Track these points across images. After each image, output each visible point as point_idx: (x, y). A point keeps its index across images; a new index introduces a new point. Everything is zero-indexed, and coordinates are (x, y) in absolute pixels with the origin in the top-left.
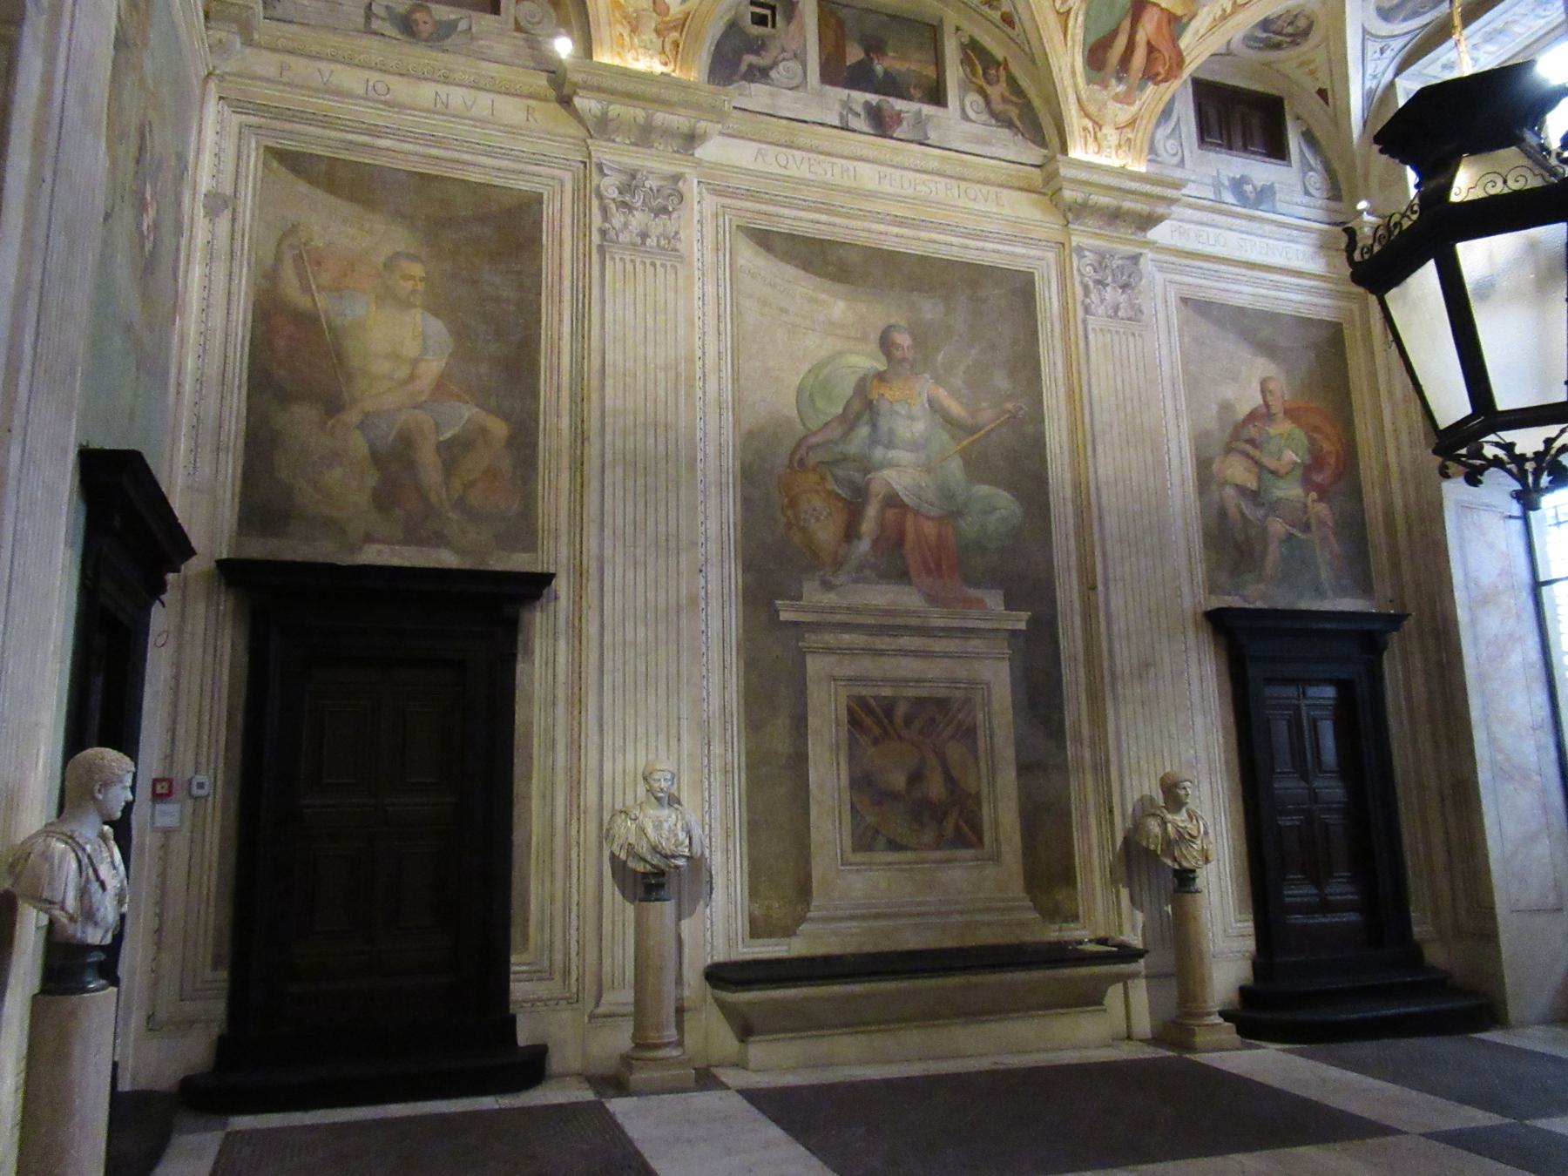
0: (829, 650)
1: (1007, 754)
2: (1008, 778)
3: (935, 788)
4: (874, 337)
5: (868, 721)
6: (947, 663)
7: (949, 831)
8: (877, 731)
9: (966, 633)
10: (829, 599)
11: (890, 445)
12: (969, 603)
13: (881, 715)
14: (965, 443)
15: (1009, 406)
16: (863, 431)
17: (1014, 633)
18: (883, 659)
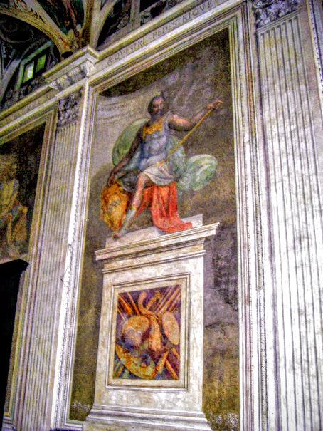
0: (114, 271)
1: (198, 315)
2: (198, 334)
3: (155, 343)
4: (146, 108)
5: (127, 306)
6: (167, 266)
7: (161, 368)
8: (130, 311)
9: (179, 246)
10: (117, 244)
11: (150, 155)
12: (183, 227)
13: (133, 302)
14: (186, 137)
15: (211, 105)
16: (138, 155)
17: (207, 239)
18: (137, 270)
